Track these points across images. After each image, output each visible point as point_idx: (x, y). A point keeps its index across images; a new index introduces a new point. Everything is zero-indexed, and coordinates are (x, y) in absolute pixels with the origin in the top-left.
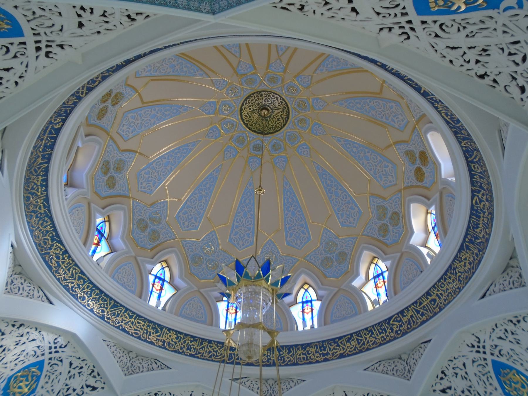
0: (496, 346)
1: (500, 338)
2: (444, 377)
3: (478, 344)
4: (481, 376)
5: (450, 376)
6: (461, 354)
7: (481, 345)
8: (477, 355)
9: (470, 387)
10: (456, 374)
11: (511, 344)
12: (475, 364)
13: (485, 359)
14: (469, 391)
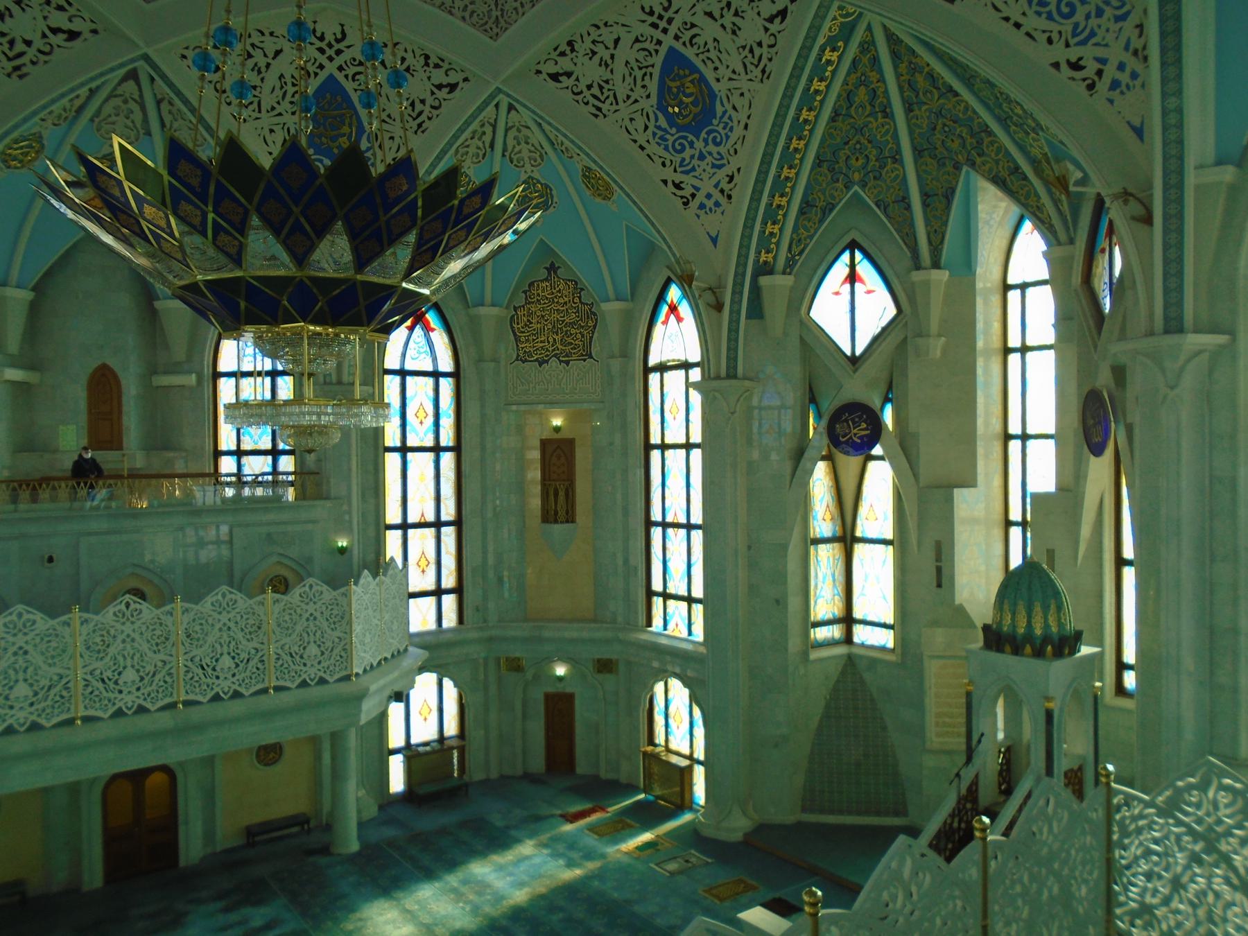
0: (693, 26)
1: (710, 15)
2: (568, 52)
3: (663, 13)
4: (636, 68)
5: (580, 55)
6: (622, 20)
7: (667, 16)
8: (650, 31)
9: (607, 82)
10: (594, 53)
11: (721, 29)
12: (638, 46)
13: (659, 43)
14: (601, 88)
